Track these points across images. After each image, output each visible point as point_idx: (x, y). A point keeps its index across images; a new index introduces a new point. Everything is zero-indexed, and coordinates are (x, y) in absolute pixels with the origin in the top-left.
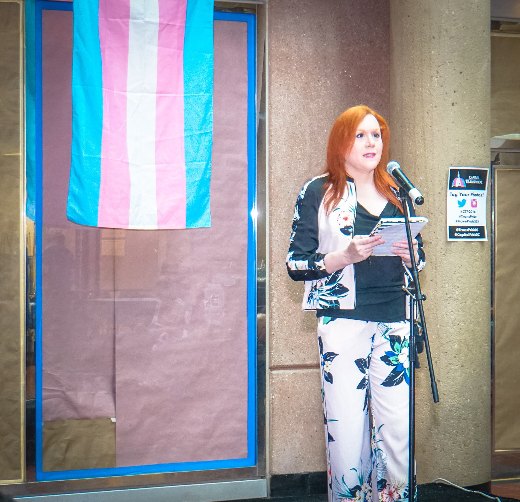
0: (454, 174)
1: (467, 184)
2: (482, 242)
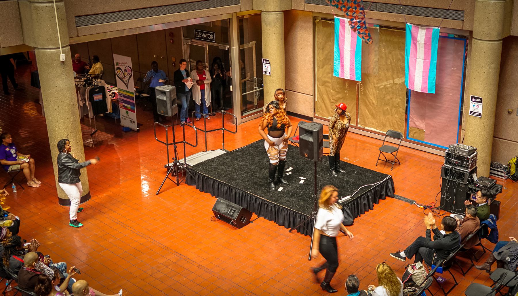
0: (472, 97)
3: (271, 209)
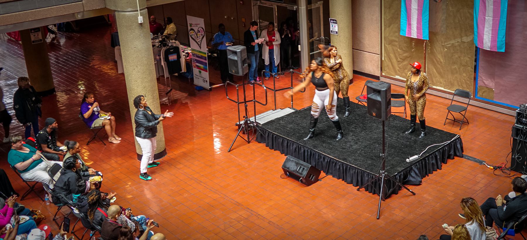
3: (340, 168)
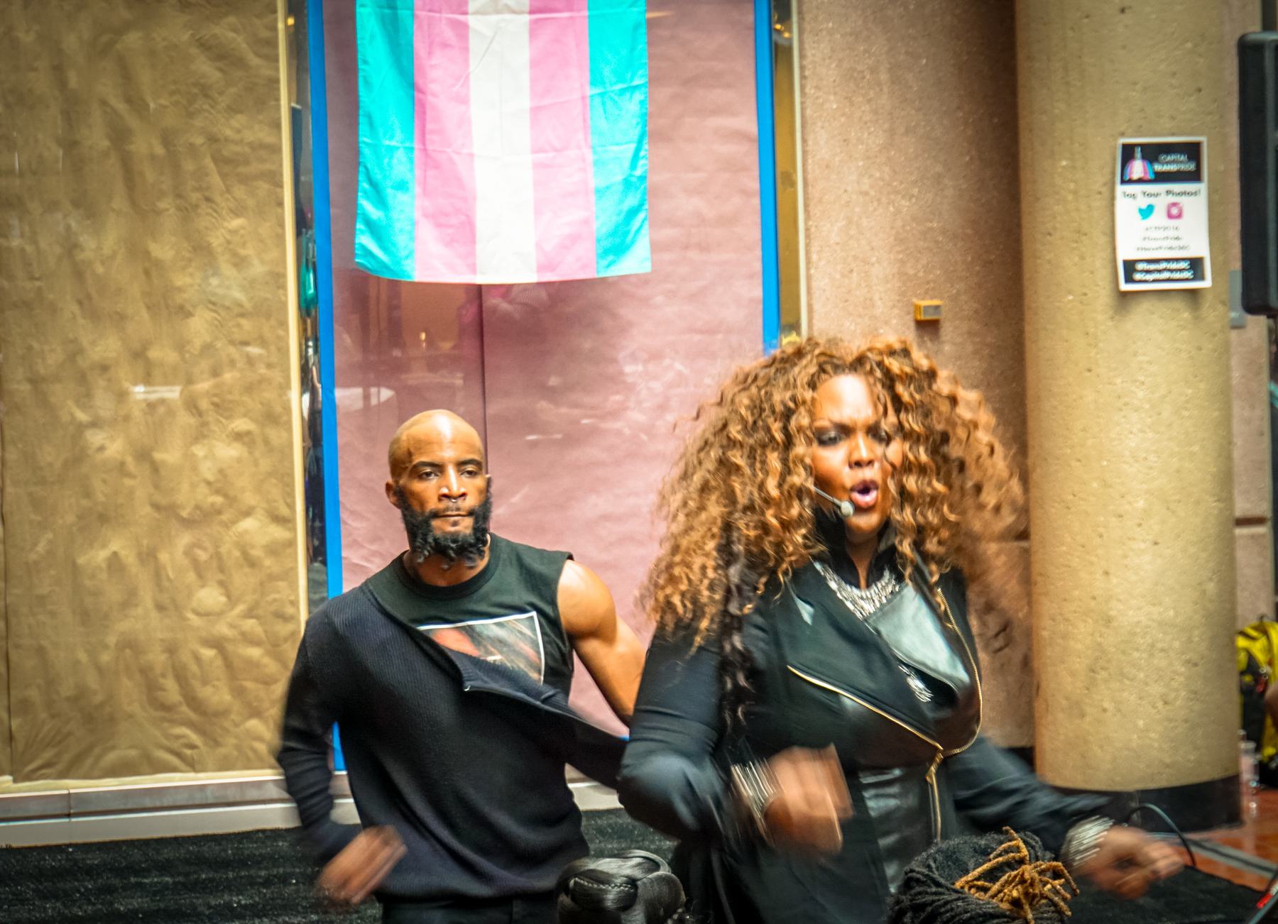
0: (1128, 153)
1: (1157, 174)
2: (1193, 293)
